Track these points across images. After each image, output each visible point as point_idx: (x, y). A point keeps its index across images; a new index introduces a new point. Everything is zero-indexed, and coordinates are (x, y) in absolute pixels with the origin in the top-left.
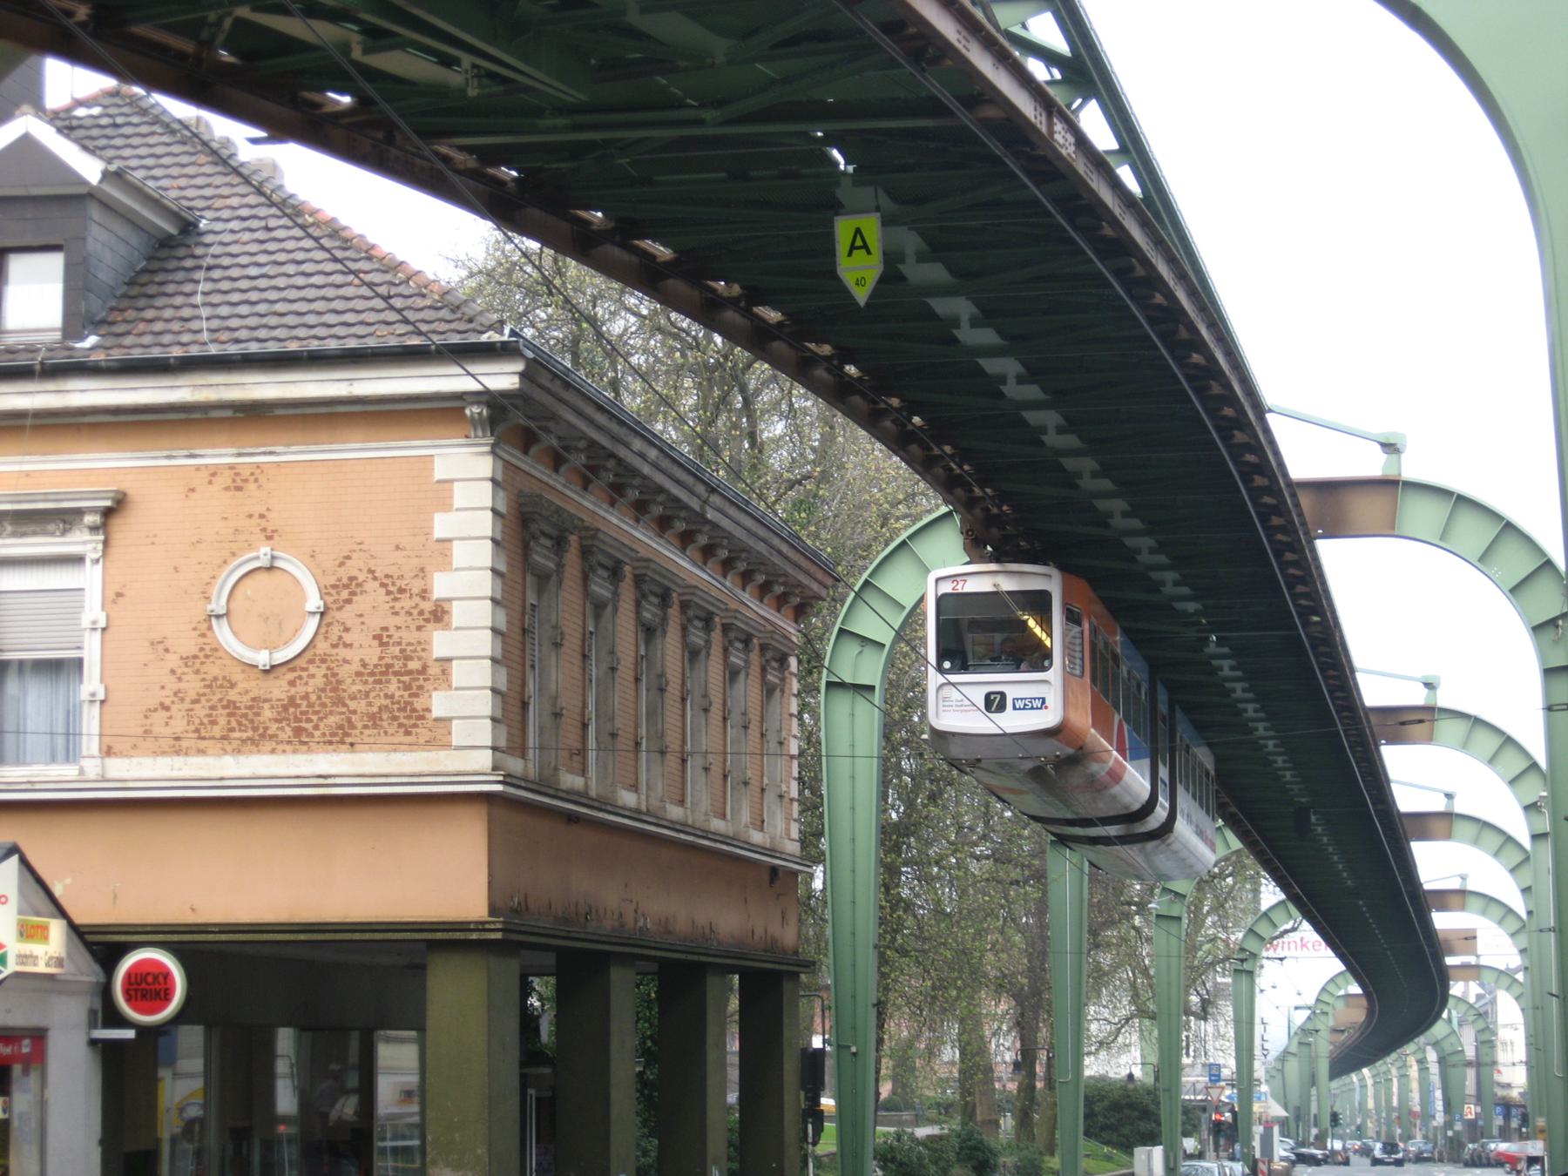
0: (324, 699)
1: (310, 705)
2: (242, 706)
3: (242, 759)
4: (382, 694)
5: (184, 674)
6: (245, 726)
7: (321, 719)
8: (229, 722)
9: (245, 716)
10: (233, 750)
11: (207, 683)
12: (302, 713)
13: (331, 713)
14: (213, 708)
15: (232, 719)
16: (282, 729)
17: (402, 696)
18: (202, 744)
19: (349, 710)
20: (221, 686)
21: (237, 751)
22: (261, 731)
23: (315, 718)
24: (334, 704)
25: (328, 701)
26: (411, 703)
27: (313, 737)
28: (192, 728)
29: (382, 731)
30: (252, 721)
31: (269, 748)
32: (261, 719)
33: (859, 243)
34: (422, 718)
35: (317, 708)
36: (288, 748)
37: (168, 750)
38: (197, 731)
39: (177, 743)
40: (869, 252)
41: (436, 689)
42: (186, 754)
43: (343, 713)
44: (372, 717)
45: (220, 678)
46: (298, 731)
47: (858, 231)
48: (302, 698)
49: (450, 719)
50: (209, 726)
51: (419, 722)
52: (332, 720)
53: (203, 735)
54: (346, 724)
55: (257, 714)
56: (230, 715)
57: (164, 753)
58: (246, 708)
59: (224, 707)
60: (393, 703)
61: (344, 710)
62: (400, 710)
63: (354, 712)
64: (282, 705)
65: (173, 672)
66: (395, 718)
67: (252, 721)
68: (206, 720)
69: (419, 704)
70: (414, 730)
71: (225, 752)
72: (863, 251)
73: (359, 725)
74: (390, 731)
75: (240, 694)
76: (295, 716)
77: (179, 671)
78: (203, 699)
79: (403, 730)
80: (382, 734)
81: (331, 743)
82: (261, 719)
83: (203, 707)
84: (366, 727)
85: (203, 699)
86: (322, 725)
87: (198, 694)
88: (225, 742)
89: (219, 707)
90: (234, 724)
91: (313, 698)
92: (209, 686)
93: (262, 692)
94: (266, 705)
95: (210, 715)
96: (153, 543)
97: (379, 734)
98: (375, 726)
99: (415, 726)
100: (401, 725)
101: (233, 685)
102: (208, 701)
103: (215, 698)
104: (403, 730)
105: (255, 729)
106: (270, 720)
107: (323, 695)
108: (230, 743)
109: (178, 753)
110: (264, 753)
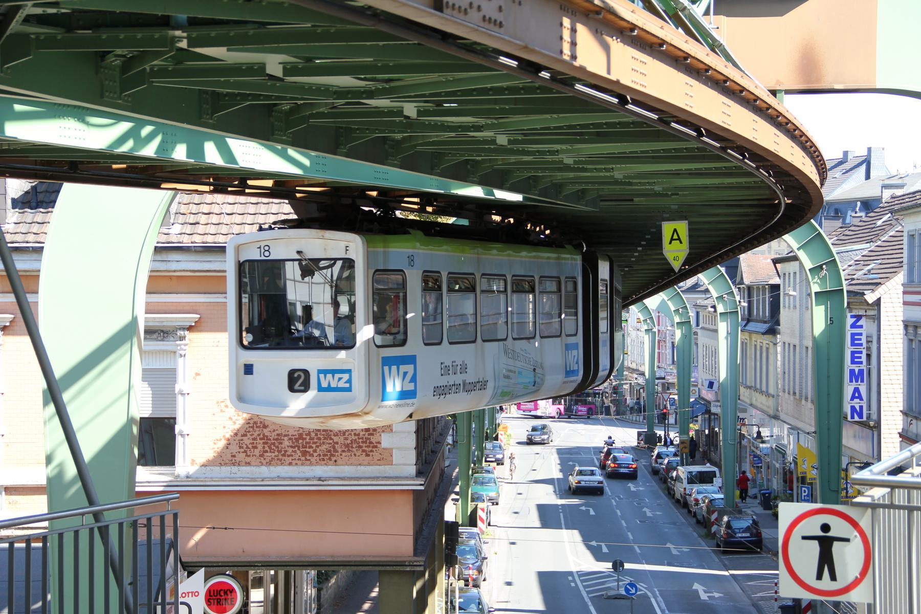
0: (319, 436)
2: (272, 438)
3: (272, 468)
4: (353, 433)
7: (317, 447)
8: (264, 447)
9: (274, 444)
10: (267, 463)
11: (250, 425)
12: (306, 443)
13: (324, 443)
14: (254, 439)
15: (266, 446)
16: (295, 452)
17: (364, 435)
18: (248, 459)
19: (333, 442)
20: (257, 427)
21: (269, 464)
23: (314, 446)
24: (325, 439)
25: (322, 437)
26: (370, 439)
28: (242, 450)
29: (353, 454)
30: (277, 447)
31: (288, 462)
32: (283, 446)
33: (675, 237)
34: (376, 447)
35: (315, 441)
36: (299, 462)
37: (227, 461)
38: (245, 452)
39: (234, 458)
40: (681, 242)
41: (383, 431)
42: (239, 465)
43: (331, 444)
44: (347, 446)
46: (304, 453)
47: (675, 230)
48: (306, 435)
49: (392, 449)
50: (252, 450)
51: (374, 449)
52: (324, 447)
55: (281, 443)
56: (264, 443)
57: (226, 464)
58: (274, 439)
59: (261, 439)
60: (359, 439)
61: (331, 441)
62: (363, 442)
63: (337, 443)
64: (295, 439)
65: (231, 418)
66: (360, 447)
67: (277, 447)
68: (250, 446)
69: (374, 439)
70: (371, 454)
71: (262, 465)
72: (678, 241)
73: (340, 450)
74: (357, 454)
75: (270, 431)
76: (303, 445)
77: (234, 418)
78: (248, 434)
80: (353, 455)
81: (324, 460)
82: (283, 446)
84: (343, 451)
85: (248, 434)
86: (318, 450)
87: (245, 431)
88: (262, 458)
89: (258, 439)
90: (267, 448)
91: (313, 435)
92: (252, 427)
93: (283, 431)
94: (286, 438)
95: (253, 443)
96: (217, 346)
98: (349, 451)
99: (372, 451)
100: (363, 451)
101: (265, 427)
103: (256, 434)
105: (279, 451)
106: (288, 446)
107: (319, 433)
108: (265, 459)
109: (234, 464)
110: (285, 465)
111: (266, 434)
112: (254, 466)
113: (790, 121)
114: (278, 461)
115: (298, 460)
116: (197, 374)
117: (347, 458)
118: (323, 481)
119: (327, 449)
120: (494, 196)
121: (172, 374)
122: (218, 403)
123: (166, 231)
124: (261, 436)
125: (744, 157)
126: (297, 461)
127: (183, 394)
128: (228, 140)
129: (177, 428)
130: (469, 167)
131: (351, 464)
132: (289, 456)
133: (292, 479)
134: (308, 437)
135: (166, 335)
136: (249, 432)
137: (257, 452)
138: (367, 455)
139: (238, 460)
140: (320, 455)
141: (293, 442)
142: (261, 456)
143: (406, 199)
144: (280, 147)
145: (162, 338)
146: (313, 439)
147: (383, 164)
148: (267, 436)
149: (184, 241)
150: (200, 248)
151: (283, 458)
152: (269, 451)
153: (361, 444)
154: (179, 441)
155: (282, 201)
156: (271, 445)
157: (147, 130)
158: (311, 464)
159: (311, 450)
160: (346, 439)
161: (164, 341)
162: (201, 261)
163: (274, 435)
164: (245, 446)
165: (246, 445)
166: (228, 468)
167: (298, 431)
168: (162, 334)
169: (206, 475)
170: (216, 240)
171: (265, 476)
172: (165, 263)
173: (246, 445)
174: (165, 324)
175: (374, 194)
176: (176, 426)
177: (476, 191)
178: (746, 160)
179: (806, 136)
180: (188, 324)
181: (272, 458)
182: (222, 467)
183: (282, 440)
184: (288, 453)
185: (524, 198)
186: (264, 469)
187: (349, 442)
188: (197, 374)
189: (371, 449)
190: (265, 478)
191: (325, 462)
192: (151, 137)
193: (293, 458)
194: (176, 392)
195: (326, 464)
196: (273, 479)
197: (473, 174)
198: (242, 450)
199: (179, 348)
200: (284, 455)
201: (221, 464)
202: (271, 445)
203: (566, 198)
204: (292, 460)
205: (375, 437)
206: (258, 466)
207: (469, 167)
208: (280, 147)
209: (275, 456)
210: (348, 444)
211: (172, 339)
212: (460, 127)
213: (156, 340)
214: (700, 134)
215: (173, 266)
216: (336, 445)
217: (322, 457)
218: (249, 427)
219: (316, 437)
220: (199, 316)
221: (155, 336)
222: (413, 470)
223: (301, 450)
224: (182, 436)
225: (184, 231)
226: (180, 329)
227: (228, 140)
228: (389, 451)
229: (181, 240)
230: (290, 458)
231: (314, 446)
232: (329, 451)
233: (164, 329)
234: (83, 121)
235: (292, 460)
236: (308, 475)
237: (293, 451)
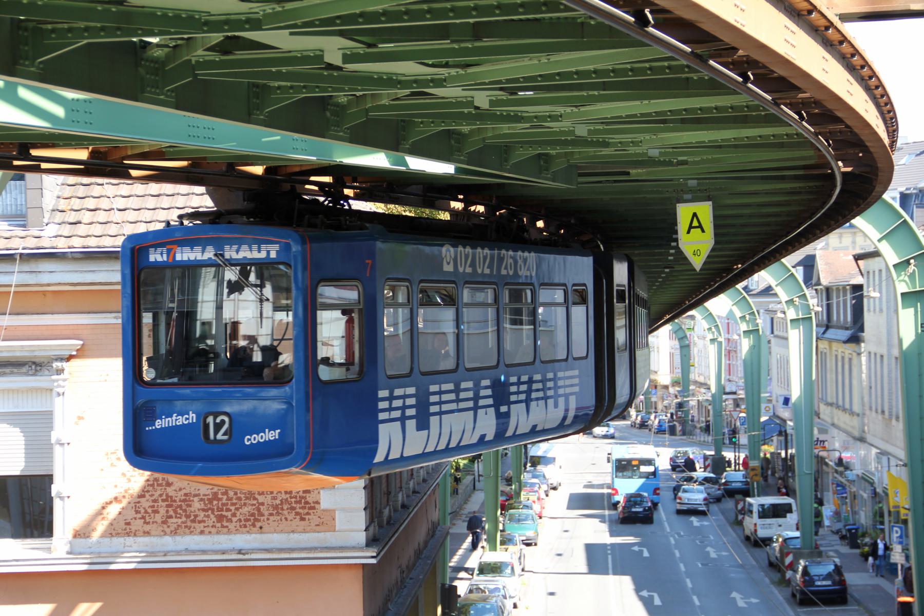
0: (239, 495)
1: (229, 499)
2: (177, 499)
3: (178, 538)
5: (132, 476)
6: (180, 514)
7: (237, 509)
8: (167, 511)
9: (180, 507)
10: (171, 532)
11: (149, 483)
12: (223, 505)
13: (245, 504)
14: (155, 501)
15: (170, 509)
16: (208, 516)
18: (147, 528)
19: (258, 503)
20: (158, 485)
21: (175, 533)
22: (192, 517)
23: (233, 508)
24: (247, 498)
25: (242, 496)
26: (305, 498)
27: (232, 522)
28: (139, 516)
29: (283, 518)
30: (185, 511)
31: (199, 530)
32: (192, 509)
34: (314, 508)
35: (234, 501)
36: (214, 530)
37: (120, 531)
38: (143, 518)
39: (128, 527)
42: (135, 535)
43: (255, 505)
44: (276, 507)
45: (160, 479)
46: (220, 518)
48: (223, 494)
49: (334, 511)
50: (152, 515)
51: (311, 511)
52: (245, 510)
53: (147, 521)
54: (256, 512)
55: (190, 506)
56: (168, 506)
57: (118, 534)
58: (180, 501)
59: (163, 501)
60: (291, 498)
61: (255, 502)
62: (296, 502)
63: (263, 504)
64: (208, 499)
65: (124, 475)
66: (293, 508)
67: (185, 511)
68: (150, 510)
69: (310, 498)
70: (307, 517)
71: (165, 534)
73: (266, 513)
74: (289, 518)
75: (175, 490)
76: (218, 508)
78: (147, 495)
79: (298, 517)
80: (284, 520)
81: (245, 526)
82: (192, 509)
83: (147, 501)
84: (271, 515)
85: (147, 495)
86: (238, 514)
87: (143, 491)
88: (165, 526)
89: (160, 501)
90: (171, 513)
92: (152, 485)
93: (193, 489)
94: (196, 499)
95: (153, 507)
96: (106, 381)
97: (281, 520)
98: (278, 514)
99: (308, 514)
102: (152, 495)
103: (157, 494)
104: (298, 517)
105: (188, 516)
106: (199, 510)
108: (169, 527)
109: (128, 534)
110: (195, 534)
111: (170, 494)
112: (154, 536)
113: (815, 7)
114: (187, 529)
115: (212, 527)
116: (80, 418)
117: (276, 524)
118: (244, 554)
119: (249, 512)
120: (406, 165)
121: (47, 418)
122: (107, 454)
123: (37, 233)
124: (164, 497)
125: (746, 79)
126: (210, 529)
127: (62, 444)
129: (55, 489)
130: (328, 114)
131: (282, 531)
132: (200, 522)
133: (204, 552)
134: (225, 497)
135: (38, 368)
136: (148, 491)
137: (158, 518)
138: (302, 519)
139: (133, 528)
140: (240, 520)
141: (205, 505)
142: (164, 522)
143: (313, 178)
145: (34, 371)
146: (231, 499)
147: (137, 100)
148: (171, 497)
149: (60, 246)
150: (78, 254)
151: (193, 525)
152: (174, 515)
153: (294, 505)
154: (57, 505)
155: (122, 181)
156: (177, 508)
158: (229, 532)
159: (229, 514)
160: (274, 498)
161: (36, 375)
162: (81, 272)
163: (180, 496)
164: (143, 511)
165: (144, 508)
166: (121, 540)
167: (212, 489)
168: (33, 367)
169: (92, 550)
170: (101, 244)
171: (169, 548)
172: (34, 275)
173: (144, 508)
174: (37, 354)
176: (53, 486)
177: (378, 160)
178: (750, 85)
179: (850, 42)
180: (67, 353)
181: (179, 526)
182: (113, 539)
183: (190, 501)
184: (199, 518)
185: (457, 169)
186: (168, 539)
187: (278, 502)
188: (80, 418)
189: (306, 511)
190: (169, 552)
191: (247, 529)
193: (206, 525)
194: (53, 441)
195: (248, 532)
196: (178, 553)
197: (258, 110)
198: (139, 516)
199: (56, 384)
200: (193, 521)
201: (111, 534)
202: (177, 508)
203: (517, 168)
204: (205, 527)
205: (312, 495)
206: (160, 536)
207: (328, 114)
209: (183, 522)
210: (277, 505)
211: (47, 373)
212: (226, 22)
213: (27, 374)
214: (642, 21)
215: (45, 279)
216: (261, 507)
217: (243, 523)
218: (148, 485)
219: (235, 497)
220: (81, 342)
221: (24, 369)
222: (361, 538)
223: (216, 513)
224: (62, 498)
225: (60, 233)
226: (56, 360)
228: (331, 513)
229: (55, 245)
230: (202, 524)
231: (233, 508)
232: (253, 515)
233: (37, 360)
235: (205, 527)
236: (225, 546)
237: (205, 516)
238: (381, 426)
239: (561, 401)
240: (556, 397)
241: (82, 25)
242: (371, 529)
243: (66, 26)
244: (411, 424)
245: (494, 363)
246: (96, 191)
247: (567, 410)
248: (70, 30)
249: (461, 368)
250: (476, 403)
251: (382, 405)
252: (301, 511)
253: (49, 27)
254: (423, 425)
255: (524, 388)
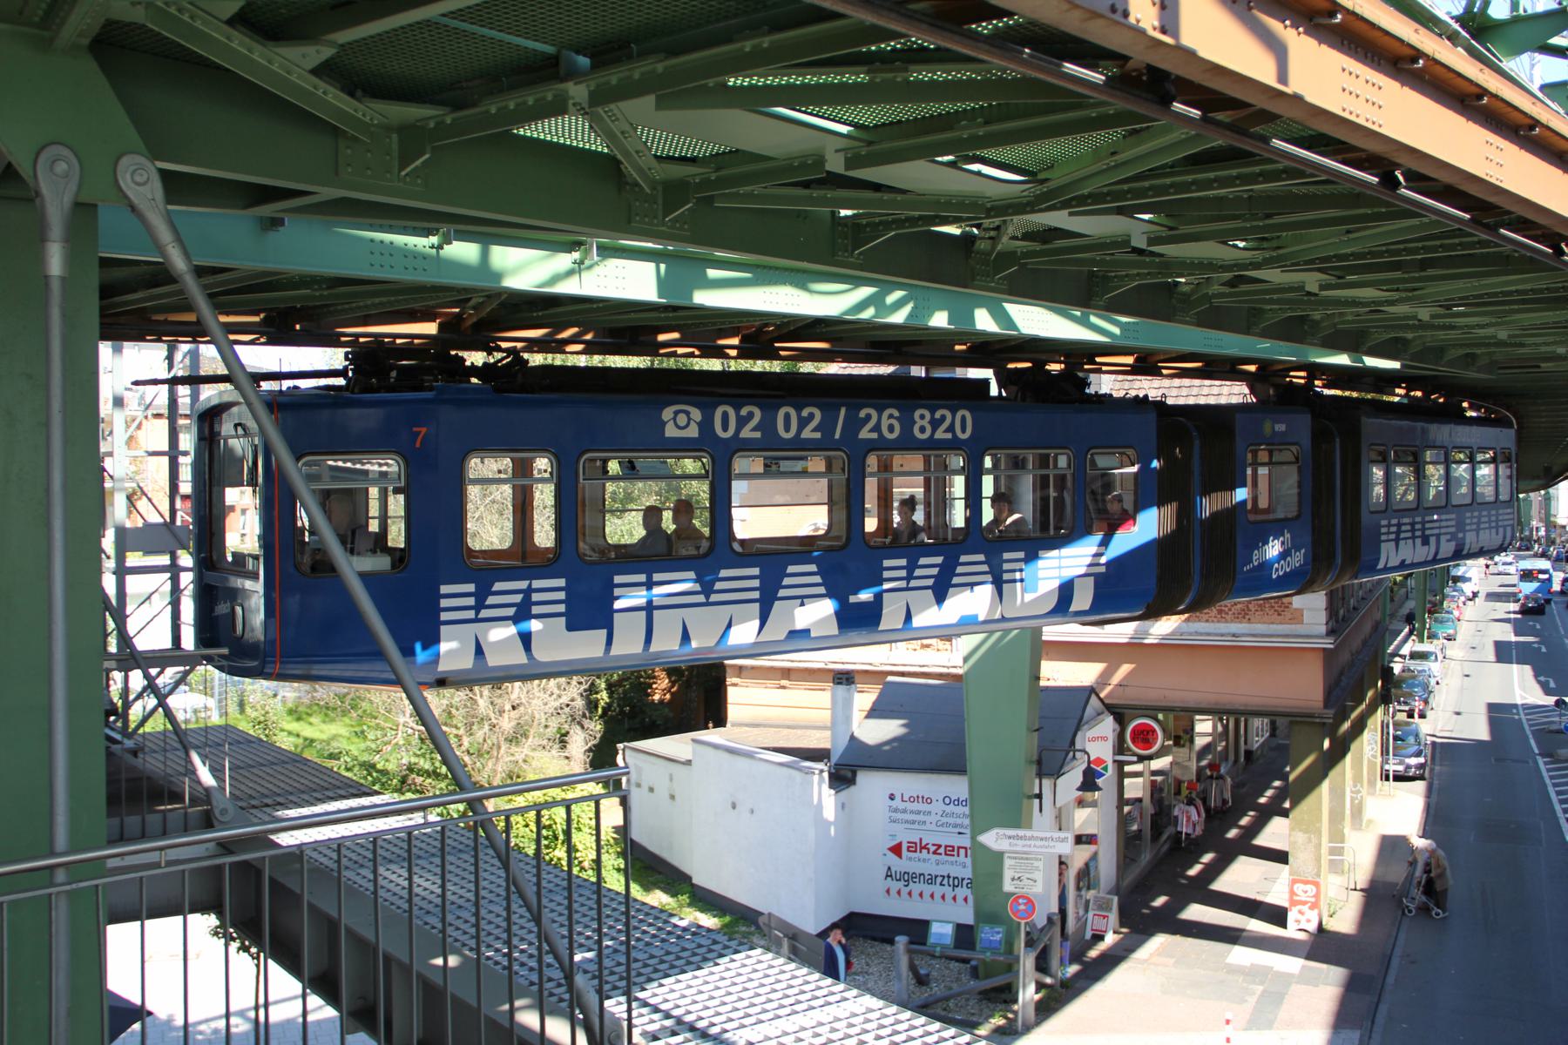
3: (1190, 624)
34: (1287, 607)
66: (1272, 607)
128: (1006, 305)
131: (1264, 623)
133: (1209, 634)
138: (1279, 615)
144: (1078, 313)
157: (891, 298)
158: (1226, 622)
175: (1252, 368)
192: (899, 305)
196: (1191, 634)
208: (1078, 313)
222: (1323, 629)
227: (1006, 305)
228: (1300, 611)
234: (804, 287)
236: (1223, 631)
238: (1383, 544)
239: (1501, 530)
240: (1497, 527)
241: (1135, 272)
242: (1330, 624)
243: (1124, 273)
244: (1418, 541)
245: (1443, 504)
246: (1205, 391)
247: (1504, 538)
248: (1127, 276)
249: (1421, 508)
250: (1478, 526)
251: (1384, 530)
252: (1279, 609)
253: (1113, 274)
254: (1426, 542)
255: (1475, 520)
